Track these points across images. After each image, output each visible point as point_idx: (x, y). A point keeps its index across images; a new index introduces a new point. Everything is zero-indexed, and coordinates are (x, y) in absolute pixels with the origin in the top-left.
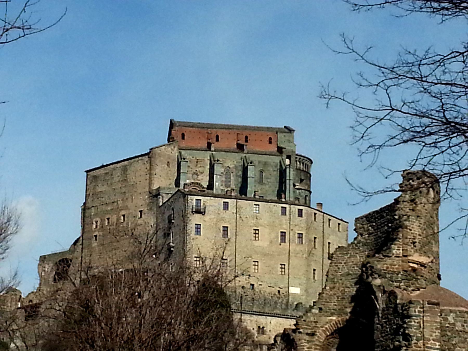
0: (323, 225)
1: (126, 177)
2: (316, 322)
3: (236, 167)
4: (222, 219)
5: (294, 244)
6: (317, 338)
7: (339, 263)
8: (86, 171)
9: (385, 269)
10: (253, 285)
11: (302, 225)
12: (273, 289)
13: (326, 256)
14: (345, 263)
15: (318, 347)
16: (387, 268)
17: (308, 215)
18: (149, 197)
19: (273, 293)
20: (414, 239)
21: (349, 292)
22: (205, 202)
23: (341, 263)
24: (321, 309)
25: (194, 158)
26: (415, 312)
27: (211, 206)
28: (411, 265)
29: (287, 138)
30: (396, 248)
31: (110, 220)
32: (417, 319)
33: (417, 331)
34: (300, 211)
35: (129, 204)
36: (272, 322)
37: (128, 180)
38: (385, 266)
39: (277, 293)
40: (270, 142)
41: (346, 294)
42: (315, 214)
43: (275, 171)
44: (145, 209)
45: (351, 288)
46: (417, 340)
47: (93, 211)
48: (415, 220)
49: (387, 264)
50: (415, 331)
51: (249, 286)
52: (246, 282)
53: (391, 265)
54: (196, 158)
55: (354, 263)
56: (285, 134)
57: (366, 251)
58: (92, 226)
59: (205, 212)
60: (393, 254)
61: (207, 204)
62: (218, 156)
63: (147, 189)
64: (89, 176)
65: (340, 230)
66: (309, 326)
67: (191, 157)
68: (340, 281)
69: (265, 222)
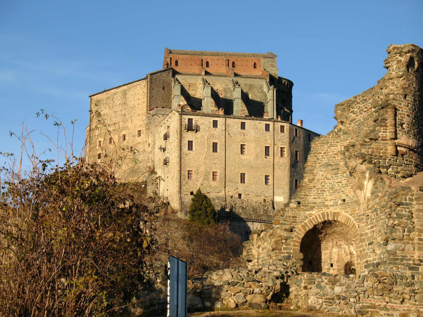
2: (293, 217)
3: (225, 90)
4: (213, 136)
5: (277, 157)
6: (296, 234)
7: (318, 154)
8: (90, 97)
9: (370, 153)
11: (285, 140)
14: (325, 153)
15: (297, 244)
16: (373, 152)
17: (291, 131)
18: (147, 118)
19: (259, 202)
20: (402, 120)
21: (330, 183)
23: (321, 153)
24: (299, 203)
25: (187, 82)
26: (406, 200)
27: (202, 124)
28: (399, 148)
29: (271, 63)
30: (382, 131)
32: (409, 208)
33: (408, 221)
34: (282, 127)
35: (129, 124)
37: (128, 103)
38: (371, 150)
39: (263, 202)
40: (255, 67)
41: (326, 186)
42: (296, 130)
44: (143, 129)
45: (332, 180)
46: (410, 231)
48: (402, 99)
49: (373, 148)
50: (405, 221)
52: (235, 192)
53: (377, 149)
54: (188, 82)
55: (335, 153)
56: (268, 59)
57: (347, 140)
60: (379, 137)
61: (199, 123)
63: (145, 110)
64: (92, 101)
66: (287, 221)
68: (321, 173)
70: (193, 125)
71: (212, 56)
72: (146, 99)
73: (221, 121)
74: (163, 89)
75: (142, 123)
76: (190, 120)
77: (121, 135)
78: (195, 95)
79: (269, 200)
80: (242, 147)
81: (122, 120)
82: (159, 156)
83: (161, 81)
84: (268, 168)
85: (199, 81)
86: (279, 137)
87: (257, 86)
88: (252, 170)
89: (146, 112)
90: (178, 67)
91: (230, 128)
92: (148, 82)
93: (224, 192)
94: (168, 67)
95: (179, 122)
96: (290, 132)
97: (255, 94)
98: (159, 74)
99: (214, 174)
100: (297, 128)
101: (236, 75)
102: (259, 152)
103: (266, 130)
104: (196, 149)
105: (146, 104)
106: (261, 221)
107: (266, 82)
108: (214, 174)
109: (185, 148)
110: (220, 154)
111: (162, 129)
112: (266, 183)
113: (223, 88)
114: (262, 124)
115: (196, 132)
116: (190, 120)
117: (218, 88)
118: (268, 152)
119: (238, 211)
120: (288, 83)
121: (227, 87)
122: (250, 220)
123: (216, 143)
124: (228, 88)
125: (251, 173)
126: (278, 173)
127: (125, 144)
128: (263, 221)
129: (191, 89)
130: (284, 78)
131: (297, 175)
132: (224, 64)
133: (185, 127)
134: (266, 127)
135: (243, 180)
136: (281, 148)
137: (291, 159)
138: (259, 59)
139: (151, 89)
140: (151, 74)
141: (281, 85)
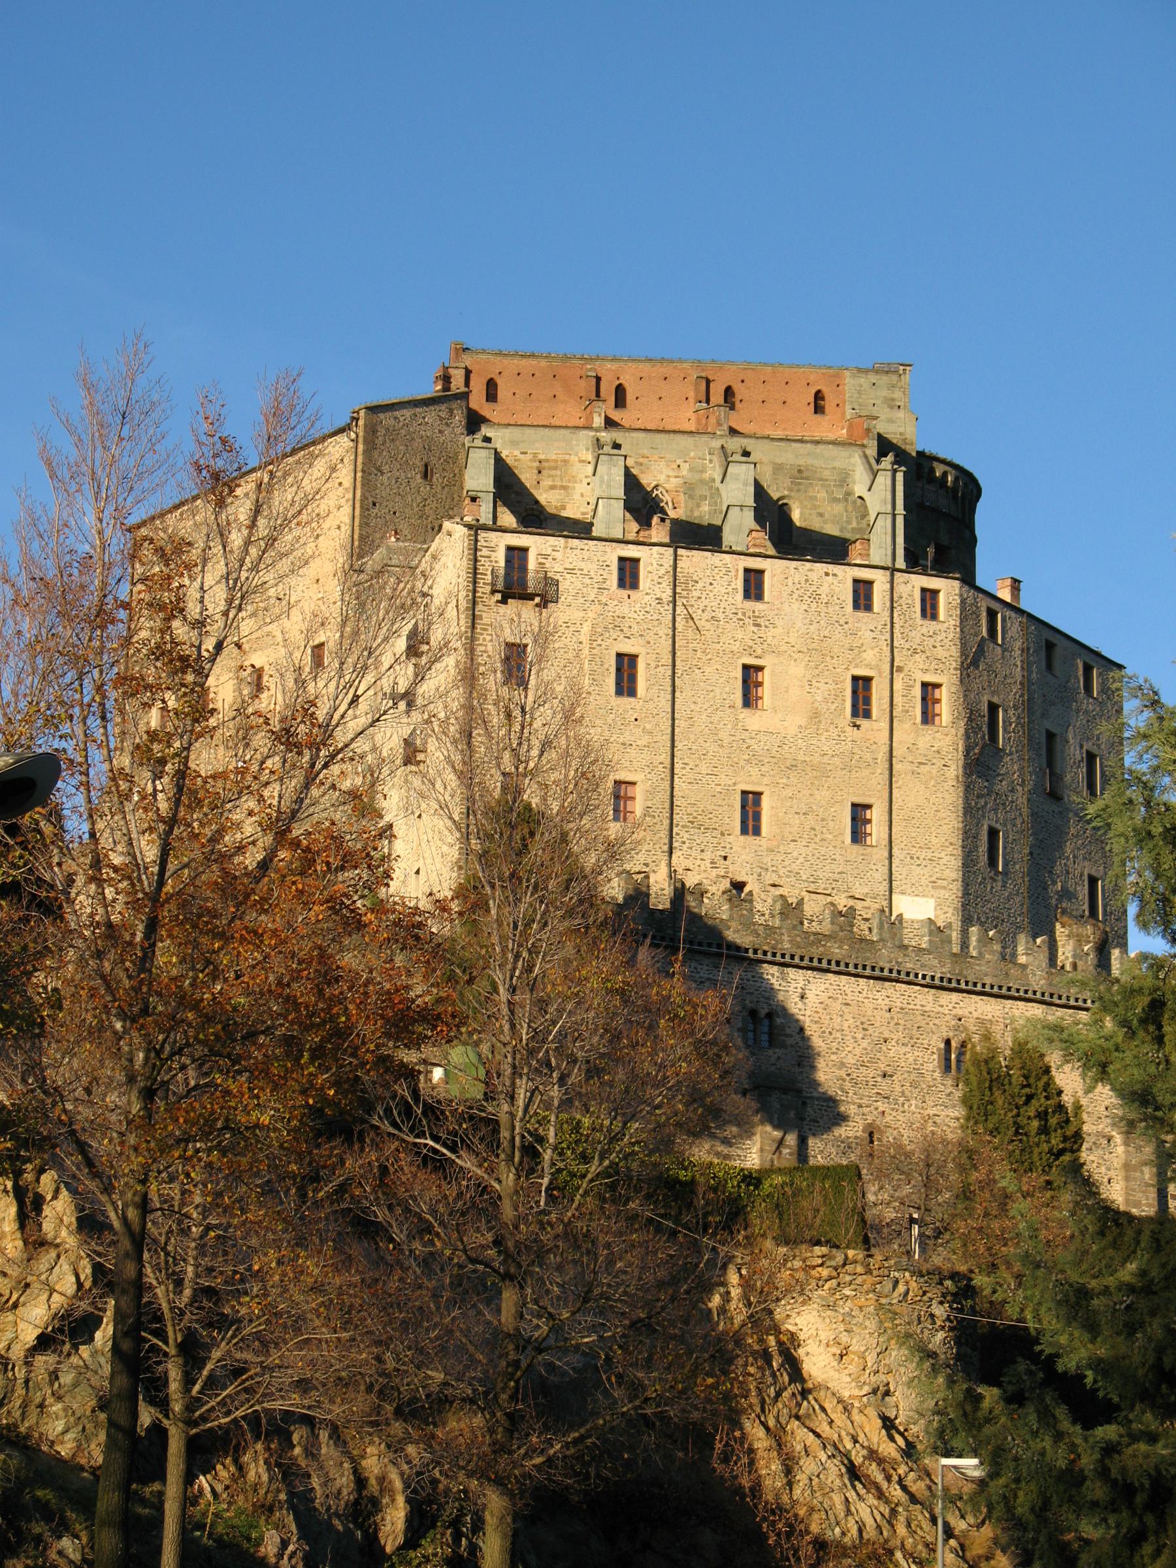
3: (689, 489)
5: (907, 726)
10: (739, 886)
11: (940, 653)
17: (966, 614)
22: (546, 556)
27: (571, 571)
29: (884, 393)
34: (929, 599)
36: (809, 994)
40: (819, 409)
42: (992, 614)
43: (838, 500)
52: (714, 872)
61: (555, 569)
67: (517, 453)
69: (792, 641)
70: (531, 575)
71: (641, 366)
72: (347, 510)
73: (654, 561)
74: (425, 476)
76: (517, 555)
78: (564, 508)
79: (868, 909)
83: (418, 443)
84: (866, 772)
85: (581, 447)
86: (916, 636)
87: (827, 474)
88: (794, 780)
90: (497, 407)
91: (696, 594)
92: (355, 441)
94: (446, 388)
95: (465, 562)
96: (963, 619)
97: (815, 507)
98: (407, 413)
100: (995, 606)
101: (733, 432)
102: (826, 700)
103: (856, 606)
106: (824, 965)
107: (866, 456)
109: (492, 681)
110: (651, 705)
112: (858, 836)
114: (836, 581)
115: (544, 604)
116: (517, 555)
117: (662, 478)
118: (867, 701)
119: (715, 906)
120: (956, 479)
121: (697, 476)
122: (769, 957)
123: (633, 658)
124: (702, 481)
125: (788, 792)
126: (909, 793)
128: (833, 967)
129: (546, 483)
130: (942, 455)
131: (995, 810)
132: (691, 395)
133: (493, 584)
134: (855, 591)
135: (750, 822)
136: (925, 685)
137: (967, 736)
138: (837, 376)
139: (369, 471)
140: (373, 410)
141: (931, 488)
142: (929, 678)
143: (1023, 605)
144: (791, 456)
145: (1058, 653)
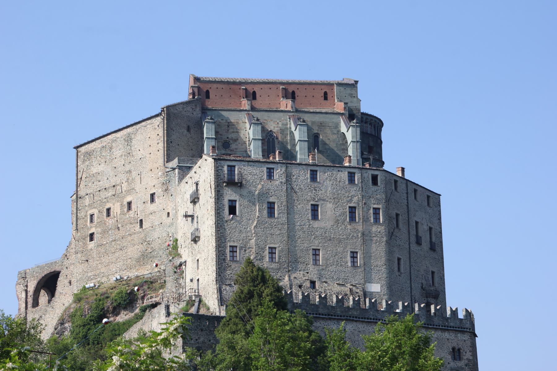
0: (407, 197)
1: (131, 149)
8: (75, 148)
12: (343, 288)
13: (413, 239)
17: (387, 183)
27: (250, 174)
31: (112, 210)
35: (138, 187)
39: (348, 293)
40: (326, 98)
42: (396, 182)
44: (159, 191)
47: (87, 201)
51: (308, 284)
58: (86, 221)
59: (241, 183)
62: (255, 114)
63: (161, 161)
64: (79, 154)
65: (431, 205)
72: (161, 145)
75: (155, 182)
76: (231, 169)
77: (125, 203)
80: (315, 209)
81: (125, 179)
82: (184, 230)
84: (355, 241)
89: (162, 165)
93: (287, 278)
94: (194, 97)
97: (326, 136)
99: (272, 251)
104: (240, 211)
105: (162, 152)
108: (272, 251)
111: (187, 186)
112: (354, 263)
113: (279, 128)
121: (285, 127)
127: (132, 216)
140: (168, 107)
142: (375, 206)
143: (406, 177)
144: (317, 118)
145: (418, 193)
